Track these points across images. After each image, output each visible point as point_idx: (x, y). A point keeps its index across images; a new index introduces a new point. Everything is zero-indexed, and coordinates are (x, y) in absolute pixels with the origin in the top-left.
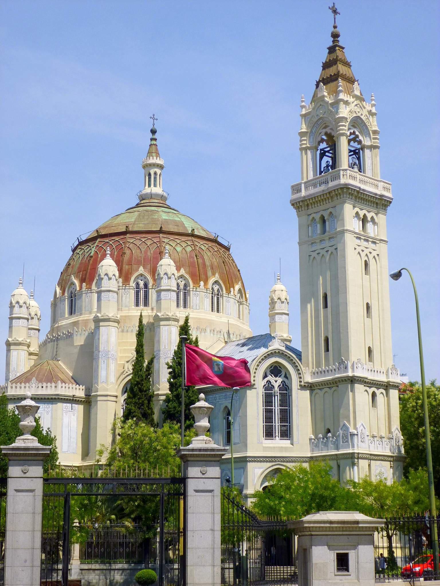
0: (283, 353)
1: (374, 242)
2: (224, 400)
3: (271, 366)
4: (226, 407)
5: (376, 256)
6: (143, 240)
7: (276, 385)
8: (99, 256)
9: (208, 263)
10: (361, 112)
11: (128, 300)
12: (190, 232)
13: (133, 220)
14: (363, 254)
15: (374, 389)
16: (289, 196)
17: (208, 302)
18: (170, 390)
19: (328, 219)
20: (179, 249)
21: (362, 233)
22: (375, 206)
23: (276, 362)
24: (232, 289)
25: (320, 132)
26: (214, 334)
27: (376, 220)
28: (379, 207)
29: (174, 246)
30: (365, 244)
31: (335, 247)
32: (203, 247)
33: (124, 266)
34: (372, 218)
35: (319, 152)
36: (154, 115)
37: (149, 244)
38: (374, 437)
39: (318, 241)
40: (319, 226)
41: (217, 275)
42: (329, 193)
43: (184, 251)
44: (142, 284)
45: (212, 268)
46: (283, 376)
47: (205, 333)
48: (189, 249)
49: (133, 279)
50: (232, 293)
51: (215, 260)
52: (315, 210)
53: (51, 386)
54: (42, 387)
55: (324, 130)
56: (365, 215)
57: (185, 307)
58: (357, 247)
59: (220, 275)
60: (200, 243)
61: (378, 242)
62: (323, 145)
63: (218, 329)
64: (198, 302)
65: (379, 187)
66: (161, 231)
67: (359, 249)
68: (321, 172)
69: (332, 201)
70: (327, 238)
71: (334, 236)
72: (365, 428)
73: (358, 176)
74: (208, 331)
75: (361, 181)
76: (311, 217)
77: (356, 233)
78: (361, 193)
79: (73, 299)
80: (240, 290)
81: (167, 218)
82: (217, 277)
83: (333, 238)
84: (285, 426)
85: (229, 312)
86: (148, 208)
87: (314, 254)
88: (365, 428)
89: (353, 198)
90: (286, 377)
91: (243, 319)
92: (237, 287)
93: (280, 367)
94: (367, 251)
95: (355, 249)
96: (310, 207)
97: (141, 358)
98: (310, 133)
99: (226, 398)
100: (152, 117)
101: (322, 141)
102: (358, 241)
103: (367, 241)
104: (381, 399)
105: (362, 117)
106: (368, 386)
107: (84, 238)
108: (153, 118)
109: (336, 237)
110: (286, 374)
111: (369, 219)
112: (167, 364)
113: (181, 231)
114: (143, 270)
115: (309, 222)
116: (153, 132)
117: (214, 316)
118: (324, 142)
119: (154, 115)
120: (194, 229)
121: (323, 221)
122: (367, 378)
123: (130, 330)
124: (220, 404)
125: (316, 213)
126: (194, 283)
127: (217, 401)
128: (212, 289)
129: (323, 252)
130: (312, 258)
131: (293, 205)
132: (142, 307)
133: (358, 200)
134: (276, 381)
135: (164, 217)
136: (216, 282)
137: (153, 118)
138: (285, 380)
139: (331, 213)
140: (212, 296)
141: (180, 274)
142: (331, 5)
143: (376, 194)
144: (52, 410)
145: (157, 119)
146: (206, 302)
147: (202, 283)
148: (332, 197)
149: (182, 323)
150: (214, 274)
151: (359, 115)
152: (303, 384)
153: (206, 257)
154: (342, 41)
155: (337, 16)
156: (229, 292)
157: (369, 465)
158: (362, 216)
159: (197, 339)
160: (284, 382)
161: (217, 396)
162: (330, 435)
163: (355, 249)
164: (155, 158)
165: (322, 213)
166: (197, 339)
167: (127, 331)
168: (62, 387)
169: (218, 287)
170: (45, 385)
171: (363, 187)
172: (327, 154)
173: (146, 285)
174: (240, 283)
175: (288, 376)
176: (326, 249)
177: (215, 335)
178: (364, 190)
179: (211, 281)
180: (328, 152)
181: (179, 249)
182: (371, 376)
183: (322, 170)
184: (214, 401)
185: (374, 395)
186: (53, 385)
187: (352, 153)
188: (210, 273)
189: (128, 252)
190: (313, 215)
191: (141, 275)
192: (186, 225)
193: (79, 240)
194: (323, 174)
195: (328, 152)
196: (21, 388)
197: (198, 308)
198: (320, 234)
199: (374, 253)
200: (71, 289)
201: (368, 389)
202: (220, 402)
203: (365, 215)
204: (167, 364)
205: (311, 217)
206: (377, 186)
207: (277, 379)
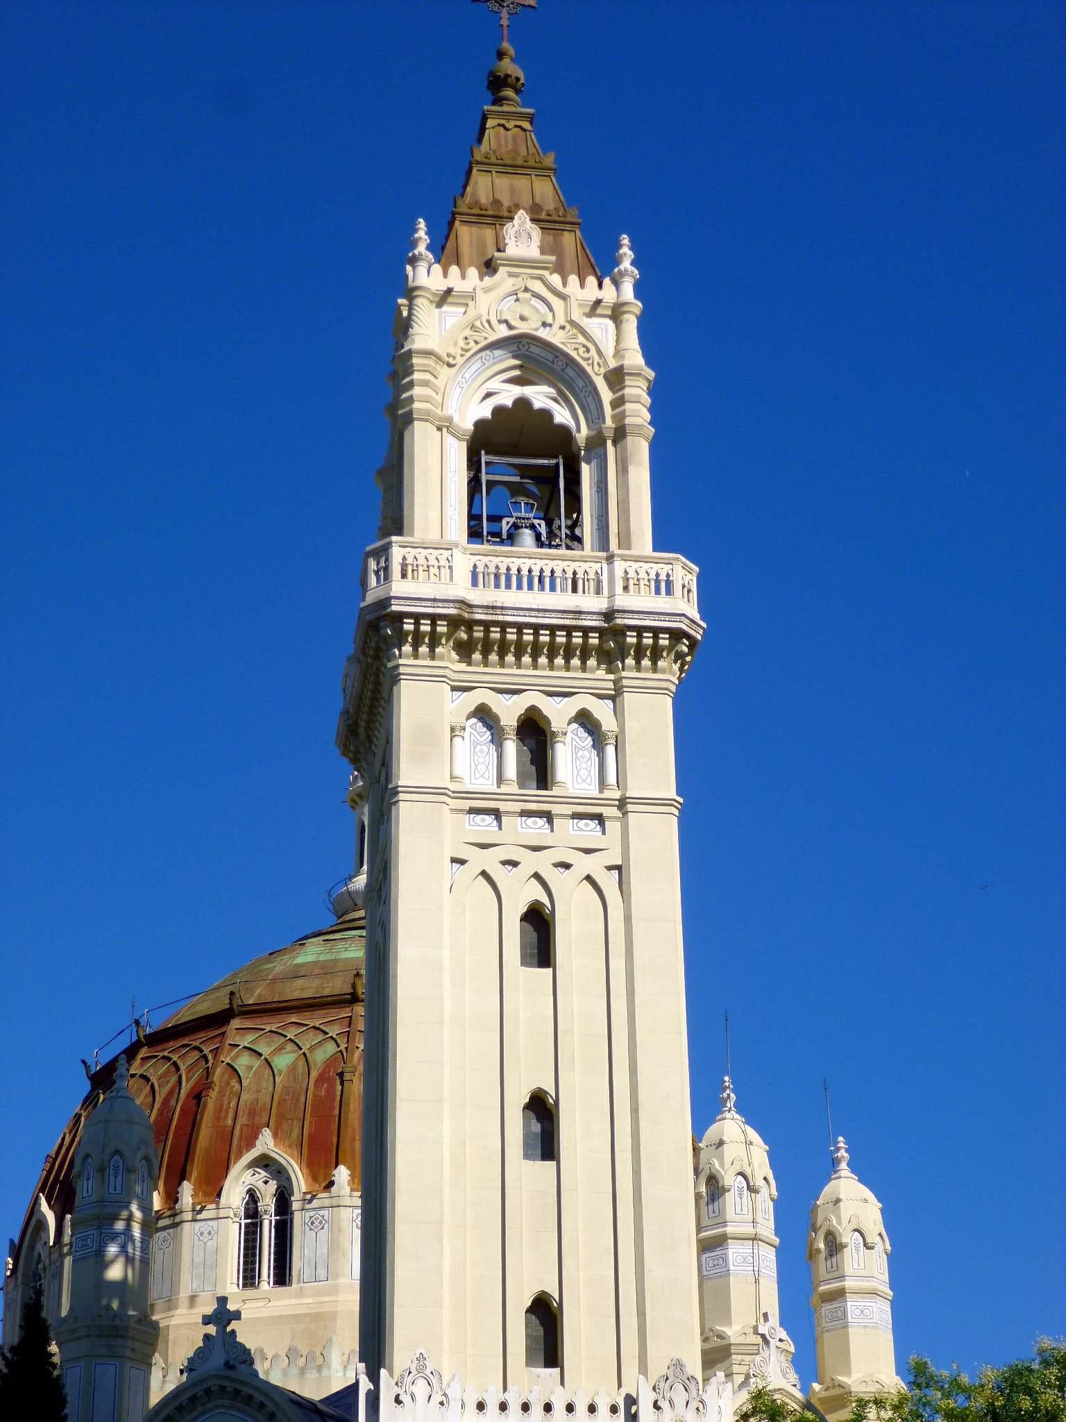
27: (608, 722)
30: (535, 829)
34: (585, 719)
78: (487, 625)
126: (314, 1177)
197: (322, 1273)
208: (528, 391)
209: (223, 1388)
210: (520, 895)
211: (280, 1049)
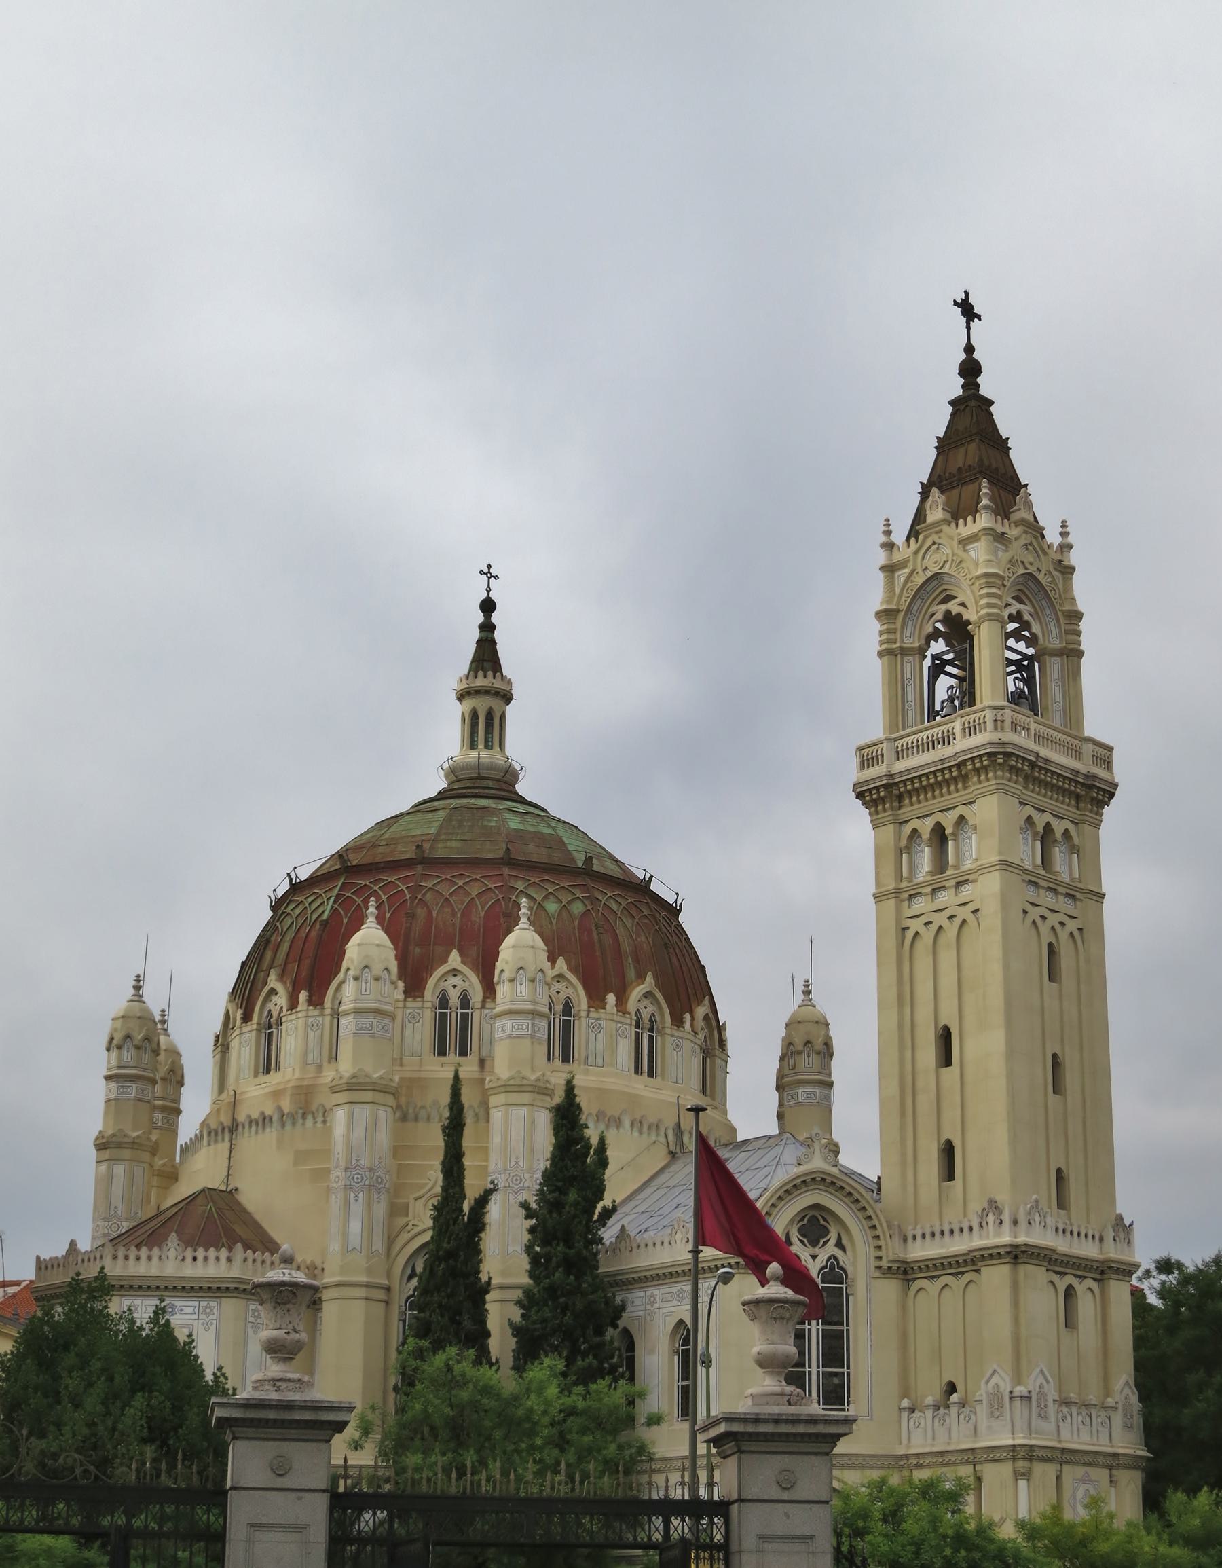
0: (833, 1183)
1: (1073, 897)
2: (676, 1303)
3: (801, 1215)
4: (681, 1322)
5: (1076, 933)
6: (461, 883)
8: (345, 921)
9: (626, 947)
10: (1037, 564)
11: (418, 1037)
12: (580, 864)
13: (433, 831)
14: (1044, 928)
15: (1069, 1279)
16: (852, 774)
17: (626, 1048)
18: (531, 1275)
19: (954, 834)
20: (552, 907)
21: (1043, 872)
22: (1073, 802)
23: (816, 1207)
24: (687, 1016)
25: (931, 610)
26: (641, 1133)
27: (1076, 841)
28: (1082, 805)
29: (539, 899)
31: (972, 907)
32: (614, 906)
33: (411, 948)
34: (1066, 832)
35: (927, 662)
36: (489, 566)
37: (474, 894)
38: (1067, 1403)
39: (929, 889)
41: (650, 979)
42: (958, 766)
43: (564, 913)
44: (454, 998)
45: (637, 960)
46: (833, 1242)
47: (618, 1128)
48: (578, 908)
49: (431, 982)
50: (687, 1026)
51: (643, 939)
52: (918, 809)
53: (217, 1259)
54: (195, 1259)
55: (943, 607)
56: (1048, 826)
57: (566, 1059)
58: (1029, 908)
59: (655, 977)
60: (607, 897)
61: (1078, 895)
62: (938, 646)
63: (652, 1119)
64: (600, 1046)
65: (1084, 756)
66: (508, 861)
67: (1034, 913)
68: (933, 714)
69: (965, 788)
70: (953, 882)
71: (971, 877)
72: (1048, 1382)
73: (1033, 726)
74: (627, 1123)
75: (1038, 738)
76: (908, 829)
77: (1026, 871)
78: (1041, 768)
79: (275, 1031)
80: (706, 1018)
81: (520, 827)
82: (649, 982)
83: (967, 881)
84: (836, 1374)
85: (680, 1076)
86: (473, 801)
87: (916, 925)
88: (1048, 1382)
89: (1021, 779)
91: (713, 1098)
92: (701, 1011)
93: (825, 1220)
94: (1053, 919)
95: (1025, 912)
96: (907, 801)
97: (457, 1189)
98: (906, 614)
99: (680, 1300)
100: (486, 570)
101: (935, 635)
102: (1031, 894)
103: (1054, 891)
104: (1086, 1306)
105: (1040, 577)
106: (1056, 1272)
107: (304, 874)
108: (488, 574)
109: (976, 881)
110: (839, 1238)
111: (1058, 834)
112: (525, 1205)
113: (558, 858)
114: (459, 959)
115: (904, 843)
116: (488, 606)
117: (641, 1085)
118: (940, 639)
119: (489, 566)
120: (591, 858)
121: (940, 836)
122: (1054, 1250)
123: (423, 1114)
124: (665, 1315)
125: (923, 817)
127: (656, 1306)
128: (638, 1013)
129: (940, 919)
130: (909, 935)
131: (860, 796)
132: (452, 1057)
133: (1031, 787)
134: (814, 1257)
135: (513, 825)
136: (647, 995)
137: (488, 574)
138: (838, 1253)
139: (962, 818)
140: (637, 1034)
141: (556, 972)
142: (960, 297)
143: (1077, 772)
144: (218, 1320)
145: (496, 577)
146: (620, 1047)
147: (611, 998)
148: (965, 778)
149: (559, 1098)
150: (641, 977)
151: (1032, 570)
152: (884, 1263)
153: (620, 931)
154: (986, 387)
155: (975, 324)
156: (678, 1022)
157: (1058, 1478)
158: (1040, 828)
159: (602, 1141)
160: (836, 1258)
161: (656, 1292)
162: (954, 1398)
163: (1025, 912)
164: (490, 673)
165: (939, 817)
166: (602, 1141)
167: (416, 1119)
168: (245, 1260)
169: (651, 1009)
170: (200, 1253)
171: (1044, 752)
172: (948, 668)
173: (465, 1002)
174: (706, 1001)
175: (844, 1242)
176: (948, 913)
177: (645, 1136)
178: (1046, 760)
179: (636, 992)
180: (951, 662)
181: (552, 907)
182: (1062, 1245)
183: (937, 708)
184: (649, 1307)
185: (1070, 1292)
186: (224, 1253)
187: (1013, 668)
188: (631, 973)
189: (421, 912)
190: (915, 824)
191: (455, 972)
192: (570, 847)
193: (291, 880)
194: (938, 718)
195: (951, 662)
196: (138, 1259)
197: (600, 1062)
198: (932, 873)
199: (1072, 926)
200: (270, 1006)
201: (1056, 1278)
202: (664, 1310)
203: (1048, 826)
204: (525, 1205)
205: (908, 829)
206: (1077, 754)
207: (817, 1250)
208: (1022, 607)
209: (824, 1180)
210: (1047, 937)
211: (546, 898)
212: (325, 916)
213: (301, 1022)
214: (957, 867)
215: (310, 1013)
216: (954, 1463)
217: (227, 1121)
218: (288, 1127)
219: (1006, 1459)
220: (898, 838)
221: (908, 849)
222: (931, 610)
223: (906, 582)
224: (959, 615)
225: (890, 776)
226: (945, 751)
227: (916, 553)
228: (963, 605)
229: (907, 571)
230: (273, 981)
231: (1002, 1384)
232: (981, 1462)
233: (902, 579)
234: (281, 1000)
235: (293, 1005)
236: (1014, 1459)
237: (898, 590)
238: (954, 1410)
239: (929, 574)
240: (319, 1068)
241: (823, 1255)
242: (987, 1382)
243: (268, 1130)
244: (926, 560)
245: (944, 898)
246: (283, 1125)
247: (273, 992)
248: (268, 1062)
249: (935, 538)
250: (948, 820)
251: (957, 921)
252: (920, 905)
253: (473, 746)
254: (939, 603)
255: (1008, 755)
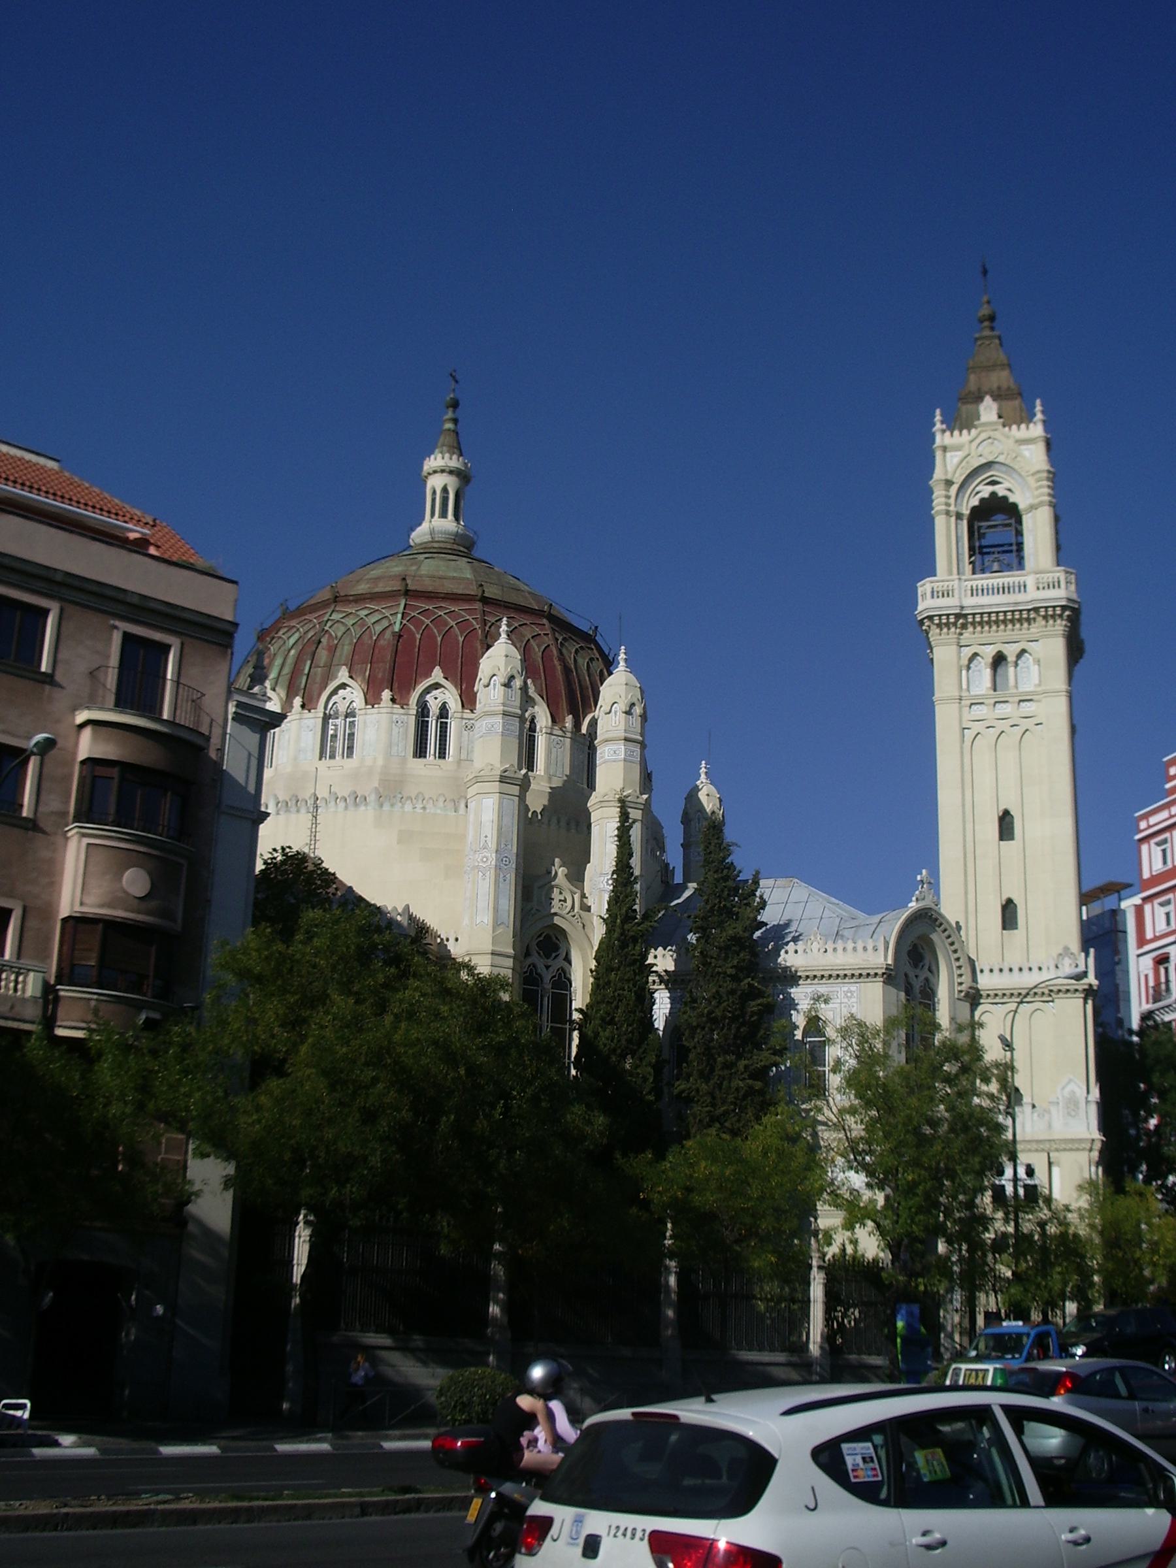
7: (917, 985)
25: (978, 489)
40: (988, 672)
42: (1029, 610)
55: (990, 488)
76: (967, 652)
87: (977, 727)
90: (930, 970)
109: (1038, 701)
139: (1023, 651)
175: (934, 968)
200: (334, 699)
207: (918, 971)
212: (397, 628)
213: (384, 718)
214: (1016, 687)
215: (395, 711)
216: (1030, 1150)
217: (307, 794)
218: (386, 807)
219: (1084, 1149)
220: (959, 658)
221: (968, 668)
222: (978, 489)
223: (962, 461)
224: (1005, 498)
225: (962, 608)
226: (1020, 597)
227: (971, 441)
228: (1009, 490)
229: (960, 454)
230: (343, 675)
231: (1077, 1090)
232: (1057, 1150)
233: (956, 460)
234: (354, 695)
235: (372, 699)
236: (1091, 1150)
237: (950, 468)
238: (1027, 1109)
239: (983, 461)
240: (404, 758)
241: (922, 978)
242: (1063, 1088)
243: (363, 808)
244: (980, 448)
245: (1004, 710)
246: (381, 806)
247: (343, 686)
248: (325, 750)
249: (992, 434)
250: (1011, 651)
251: (1018, 731)
252: (979, 712)
253: (444, 515)
254: (988, 484)
255: (1072, 609)
